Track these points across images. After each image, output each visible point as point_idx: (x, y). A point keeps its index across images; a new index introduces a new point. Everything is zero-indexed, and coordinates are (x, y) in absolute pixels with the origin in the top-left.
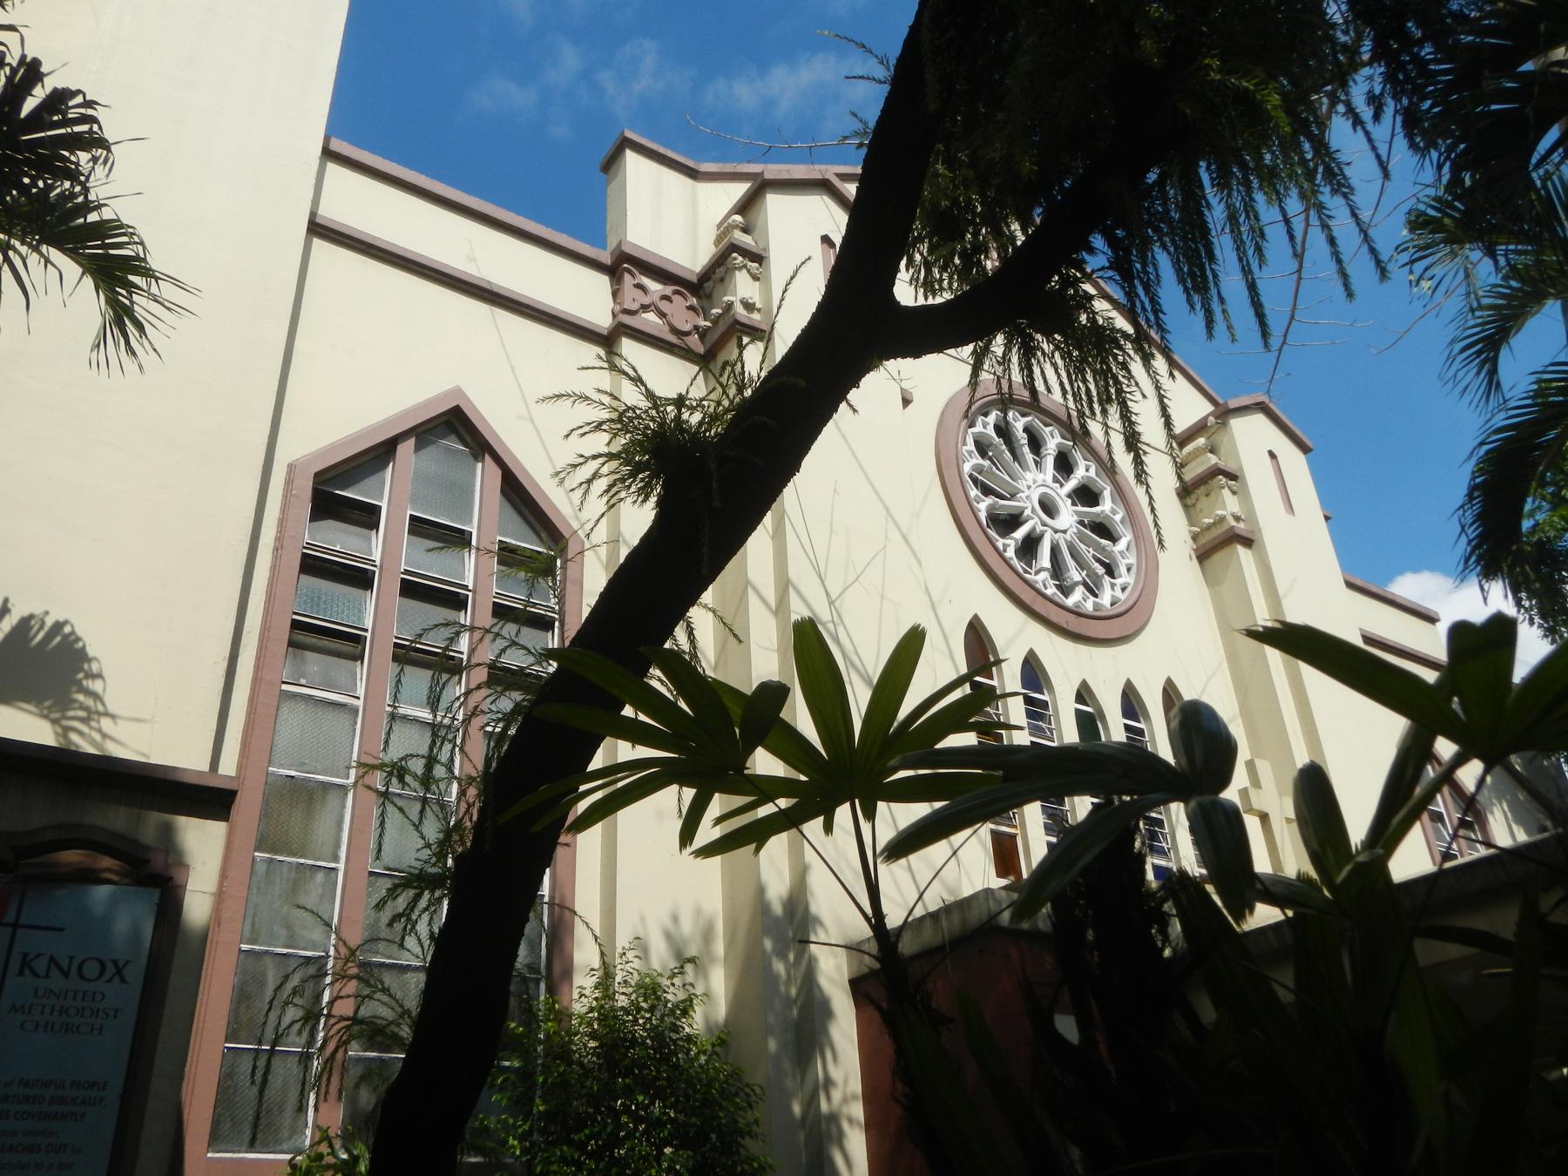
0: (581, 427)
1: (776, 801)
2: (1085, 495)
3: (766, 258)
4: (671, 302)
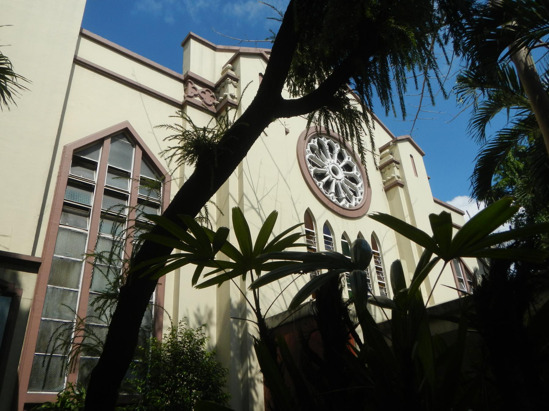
0: (169, 137)
1: (225, 270)
2: (348, 168)
3: (239, 80)
4: (205, 94)
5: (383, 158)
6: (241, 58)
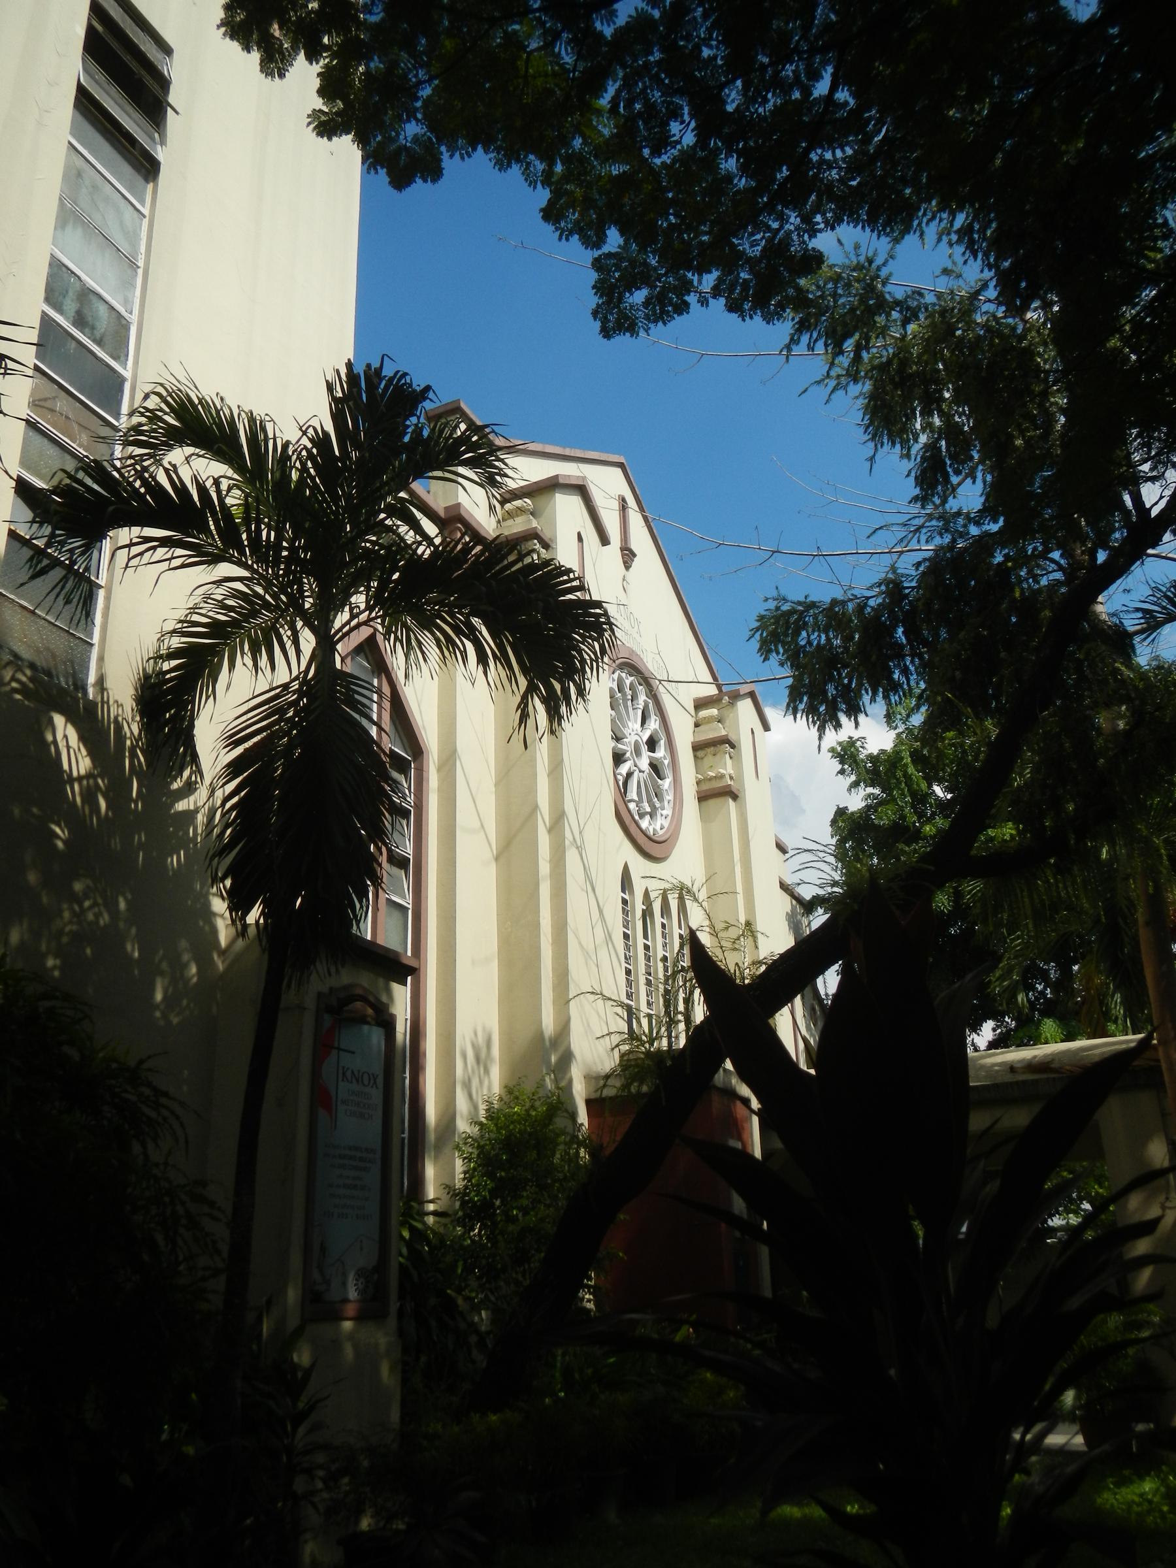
5: (702, 724)
6: (557, 494)
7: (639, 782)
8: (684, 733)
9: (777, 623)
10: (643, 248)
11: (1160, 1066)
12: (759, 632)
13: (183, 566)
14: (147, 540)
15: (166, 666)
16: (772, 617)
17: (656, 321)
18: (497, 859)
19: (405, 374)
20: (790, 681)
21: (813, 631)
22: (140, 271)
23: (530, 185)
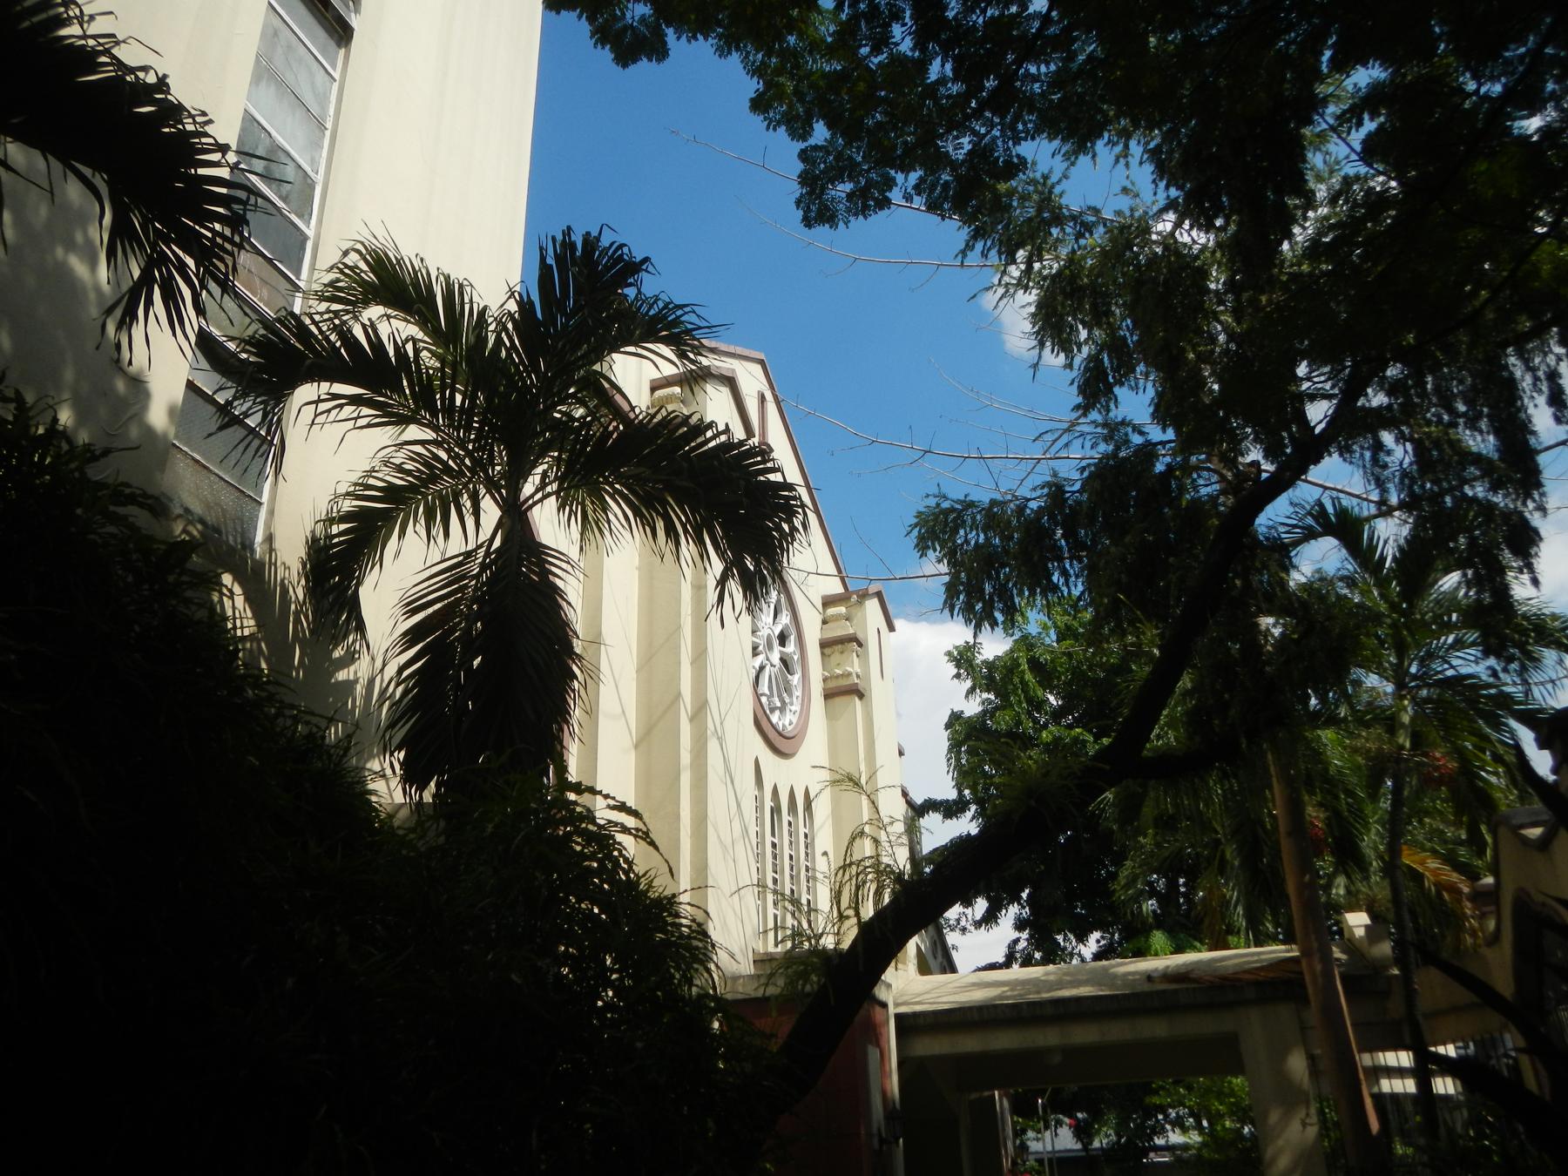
7: (770, 676)
8: (813, 632)
9: (936, 520)
10: (848, 144)
11: (1304, 979)
12: (918, 529)
13: (369, 426)
14: (335, 397)
15: (335, 529)
16: (933, 514)
17: (856, 215)
18: (636, 747)
19: (621, 246)
20: (947, 579)
21: (971, 530)
22: (328, 133)
23: (747, 74)
